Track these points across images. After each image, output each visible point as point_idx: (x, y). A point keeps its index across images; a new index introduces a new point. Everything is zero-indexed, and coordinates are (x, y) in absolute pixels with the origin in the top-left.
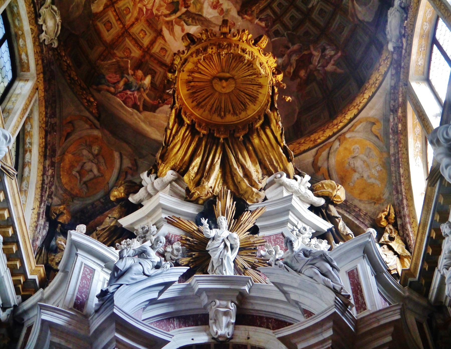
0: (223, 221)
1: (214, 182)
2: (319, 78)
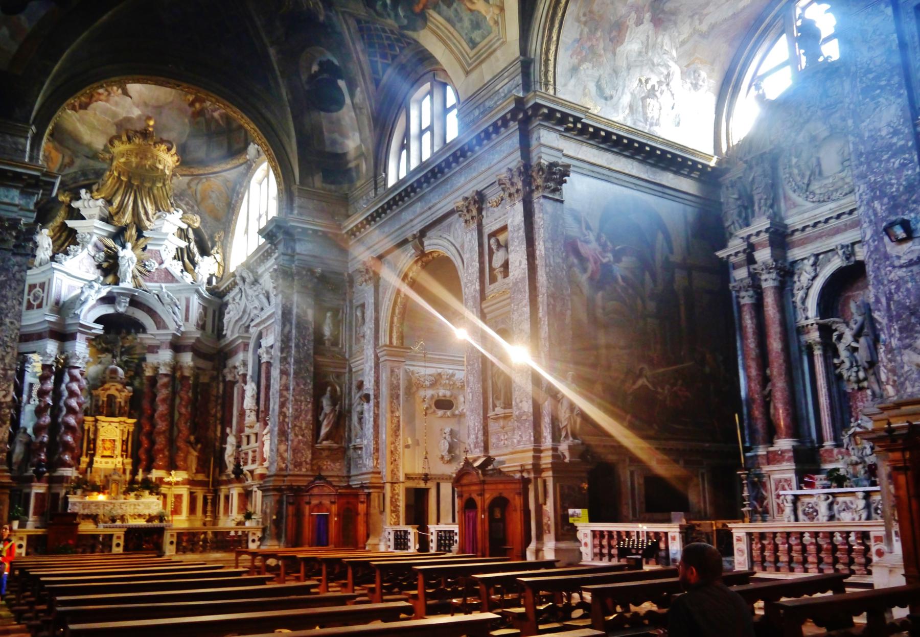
0: (129, 245)
1: (127, 218)
2: (207, 116)
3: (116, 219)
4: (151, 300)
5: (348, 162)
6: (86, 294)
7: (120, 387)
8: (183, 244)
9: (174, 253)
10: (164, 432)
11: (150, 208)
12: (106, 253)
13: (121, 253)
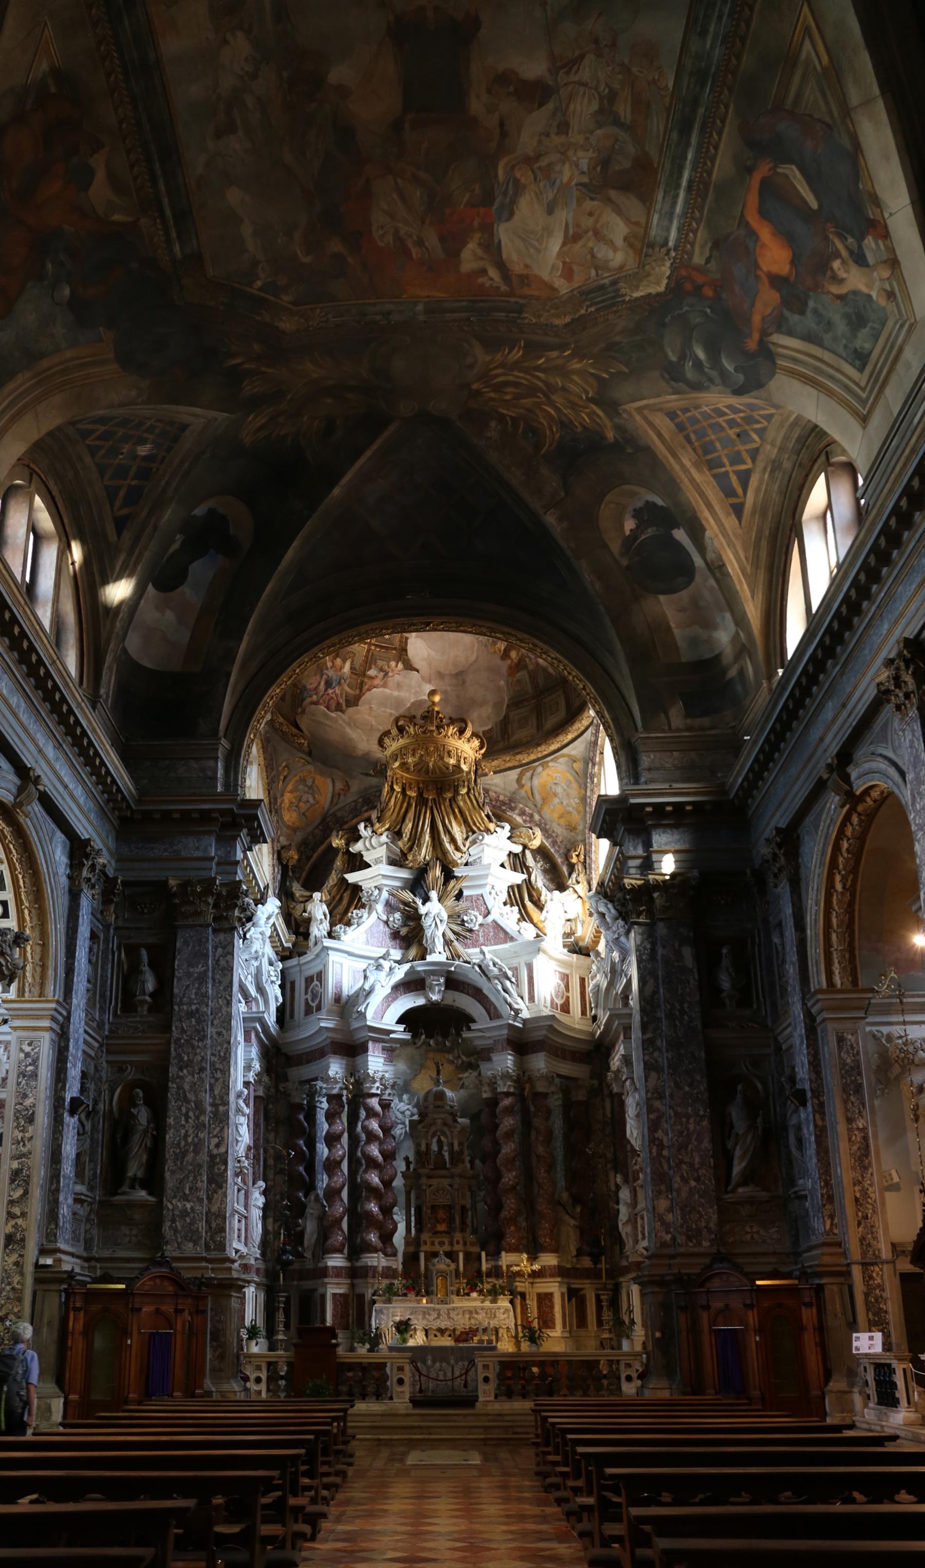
0: (434, 894)
1: (425, 852)
3: (410, 858)
4: (471, 976)
5: (724, 671)
6: (371, 980)
7: (450, 1120)
8: (518, 878)
9: (504, 896)
10: (514, 1188)
11: (458, 832)
12: (403, 913)
13: (423, 910)
